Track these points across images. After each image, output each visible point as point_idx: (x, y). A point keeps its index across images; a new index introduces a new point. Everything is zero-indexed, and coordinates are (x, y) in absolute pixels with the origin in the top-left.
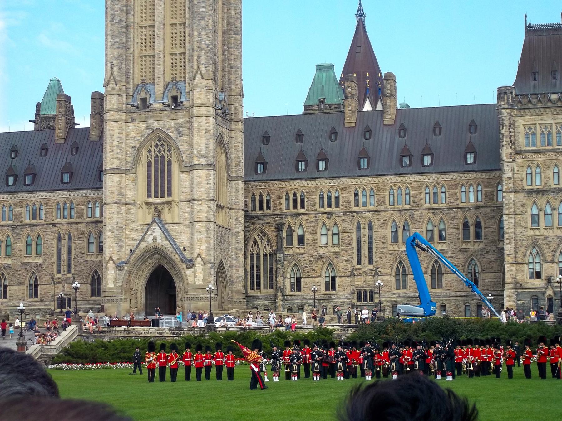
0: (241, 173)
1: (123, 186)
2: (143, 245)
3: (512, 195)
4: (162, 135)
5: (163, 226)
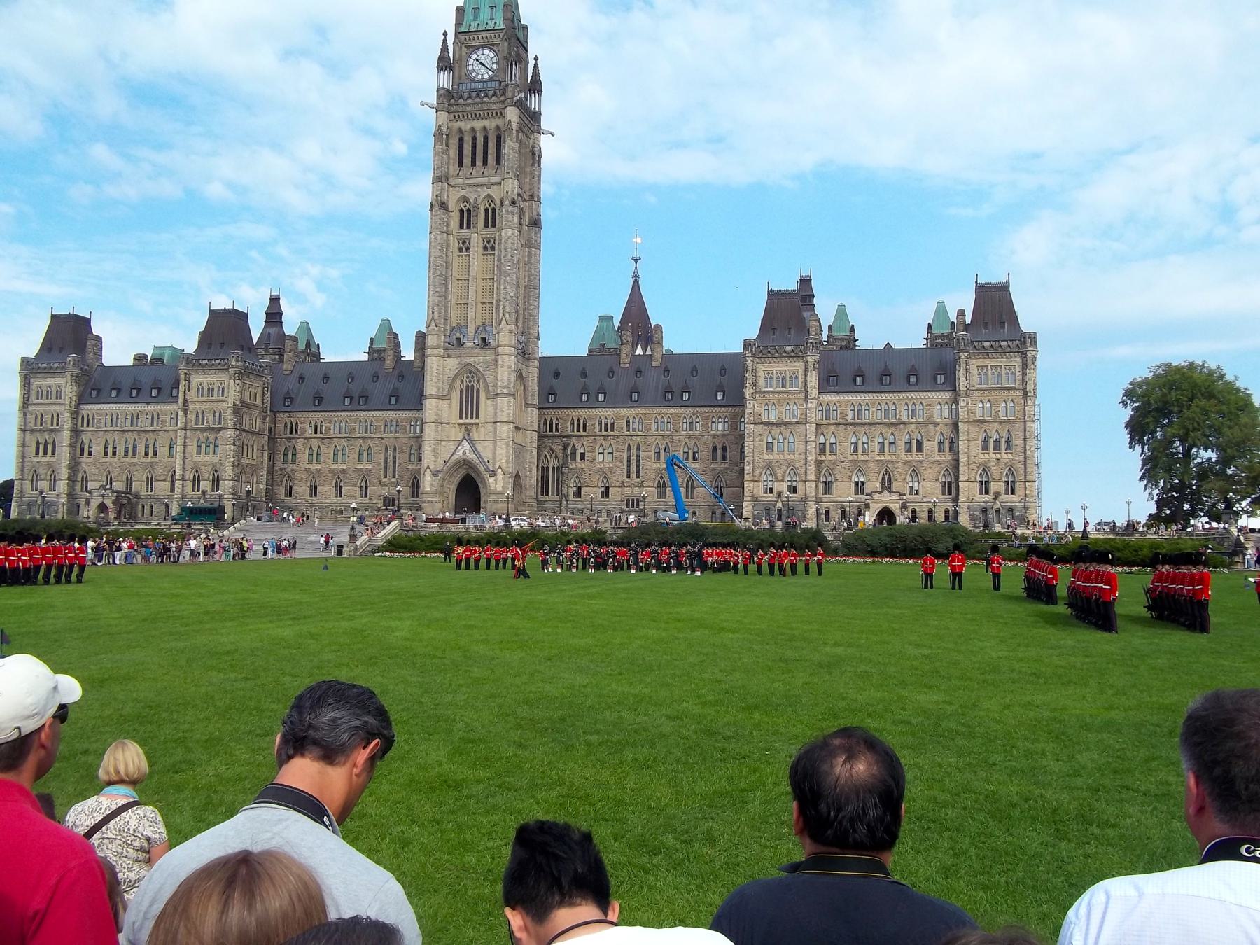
0: (536, 401)
1: (439, 408)
2: (455, 457)
3: (752, 427)
5: (472, 443)
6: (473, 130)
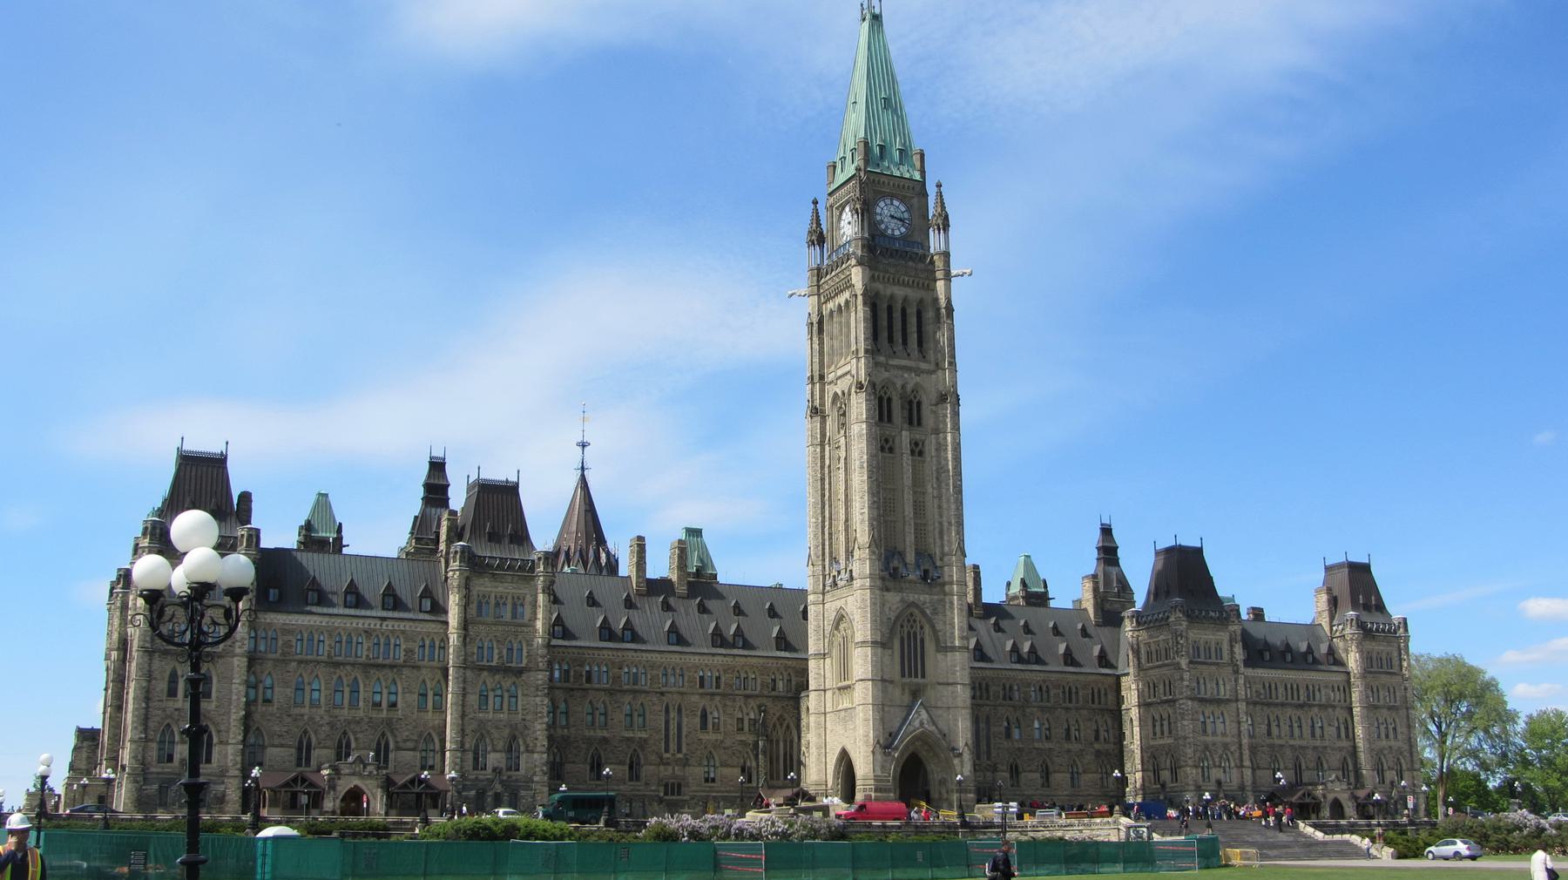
4: (916, 612)
6: (892, 297)
